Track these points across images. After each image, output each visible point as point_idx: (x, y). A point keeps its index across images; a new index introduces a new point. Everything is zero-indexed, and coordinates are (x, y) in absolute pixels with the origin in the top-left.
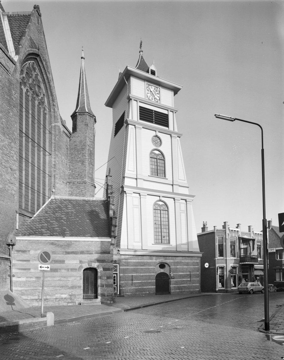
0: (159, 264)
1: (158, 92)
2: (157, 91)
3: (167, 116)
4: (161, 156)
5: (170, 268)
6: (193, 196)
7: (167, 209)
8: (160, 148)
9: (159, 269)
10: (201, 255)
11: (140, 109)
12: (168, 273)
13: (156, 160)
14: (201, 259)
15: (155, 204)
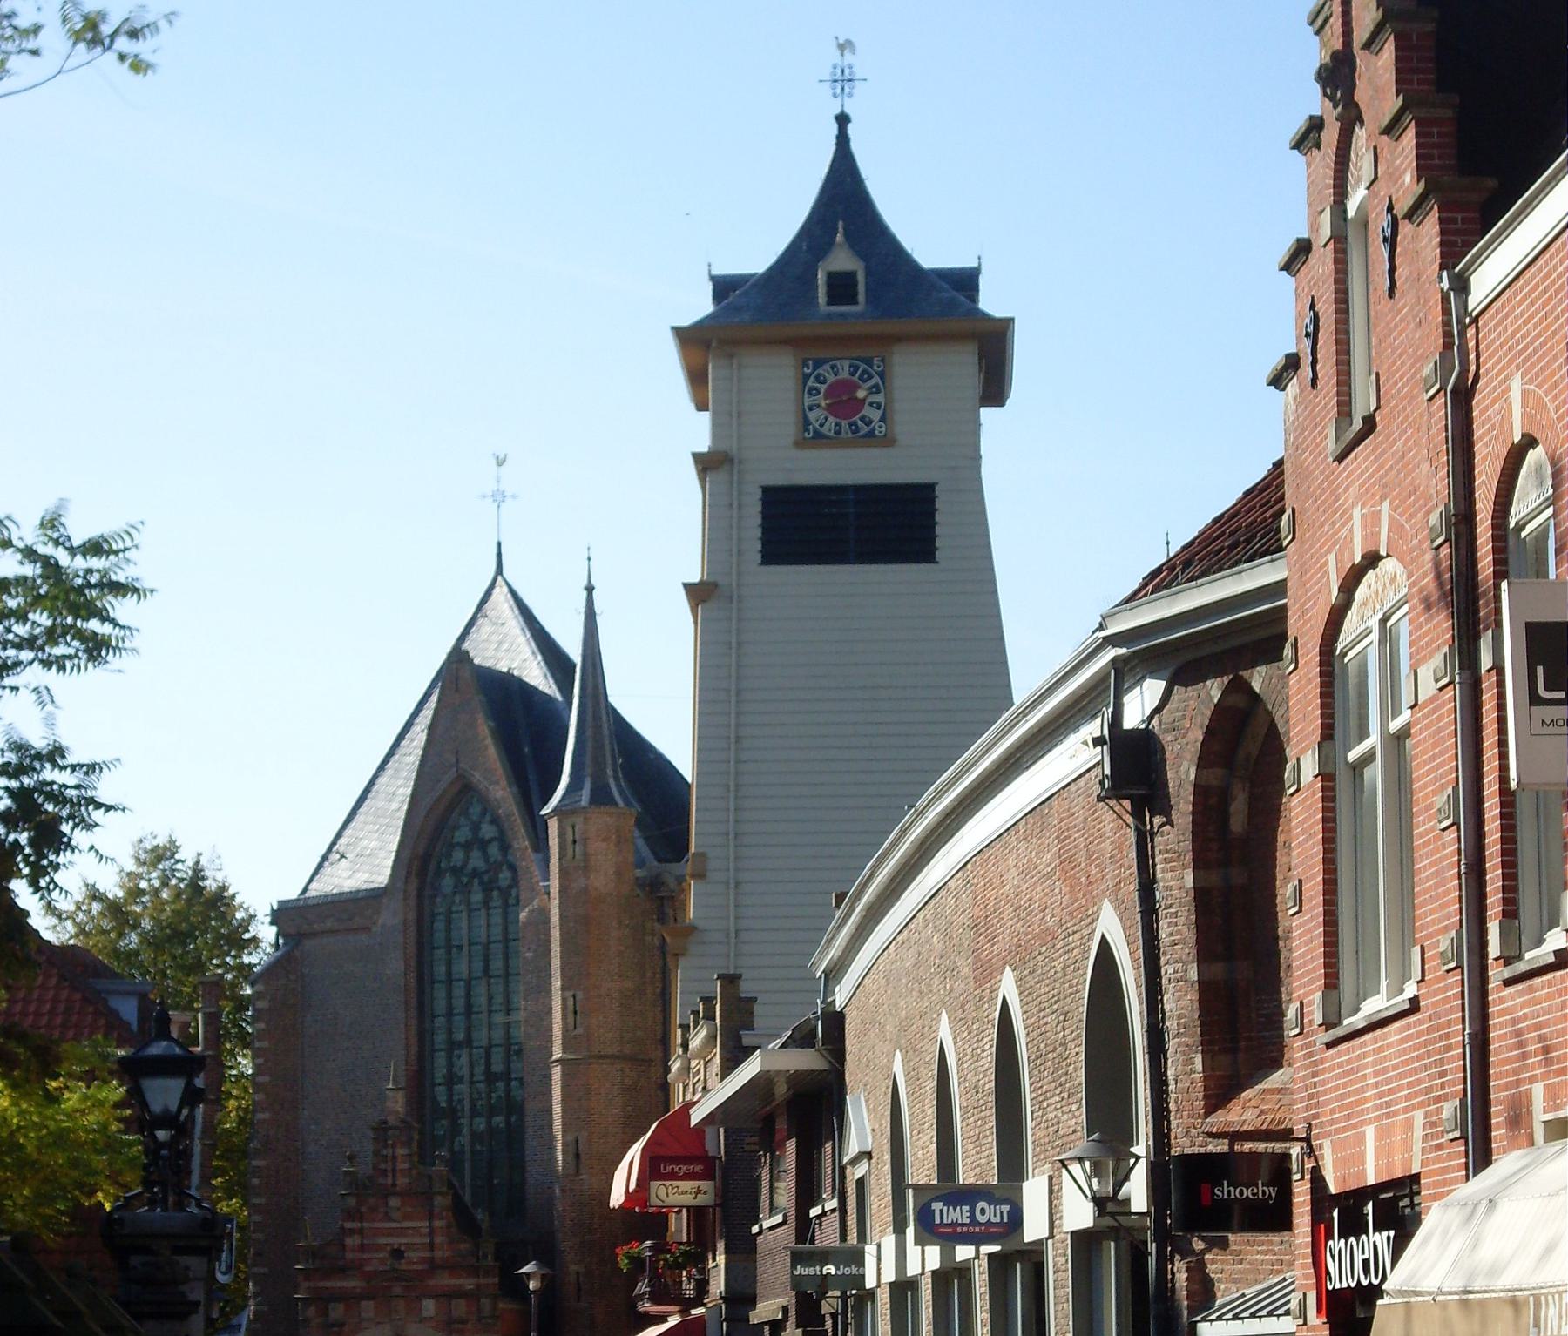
1: (876, 379)
2: (871, 377)
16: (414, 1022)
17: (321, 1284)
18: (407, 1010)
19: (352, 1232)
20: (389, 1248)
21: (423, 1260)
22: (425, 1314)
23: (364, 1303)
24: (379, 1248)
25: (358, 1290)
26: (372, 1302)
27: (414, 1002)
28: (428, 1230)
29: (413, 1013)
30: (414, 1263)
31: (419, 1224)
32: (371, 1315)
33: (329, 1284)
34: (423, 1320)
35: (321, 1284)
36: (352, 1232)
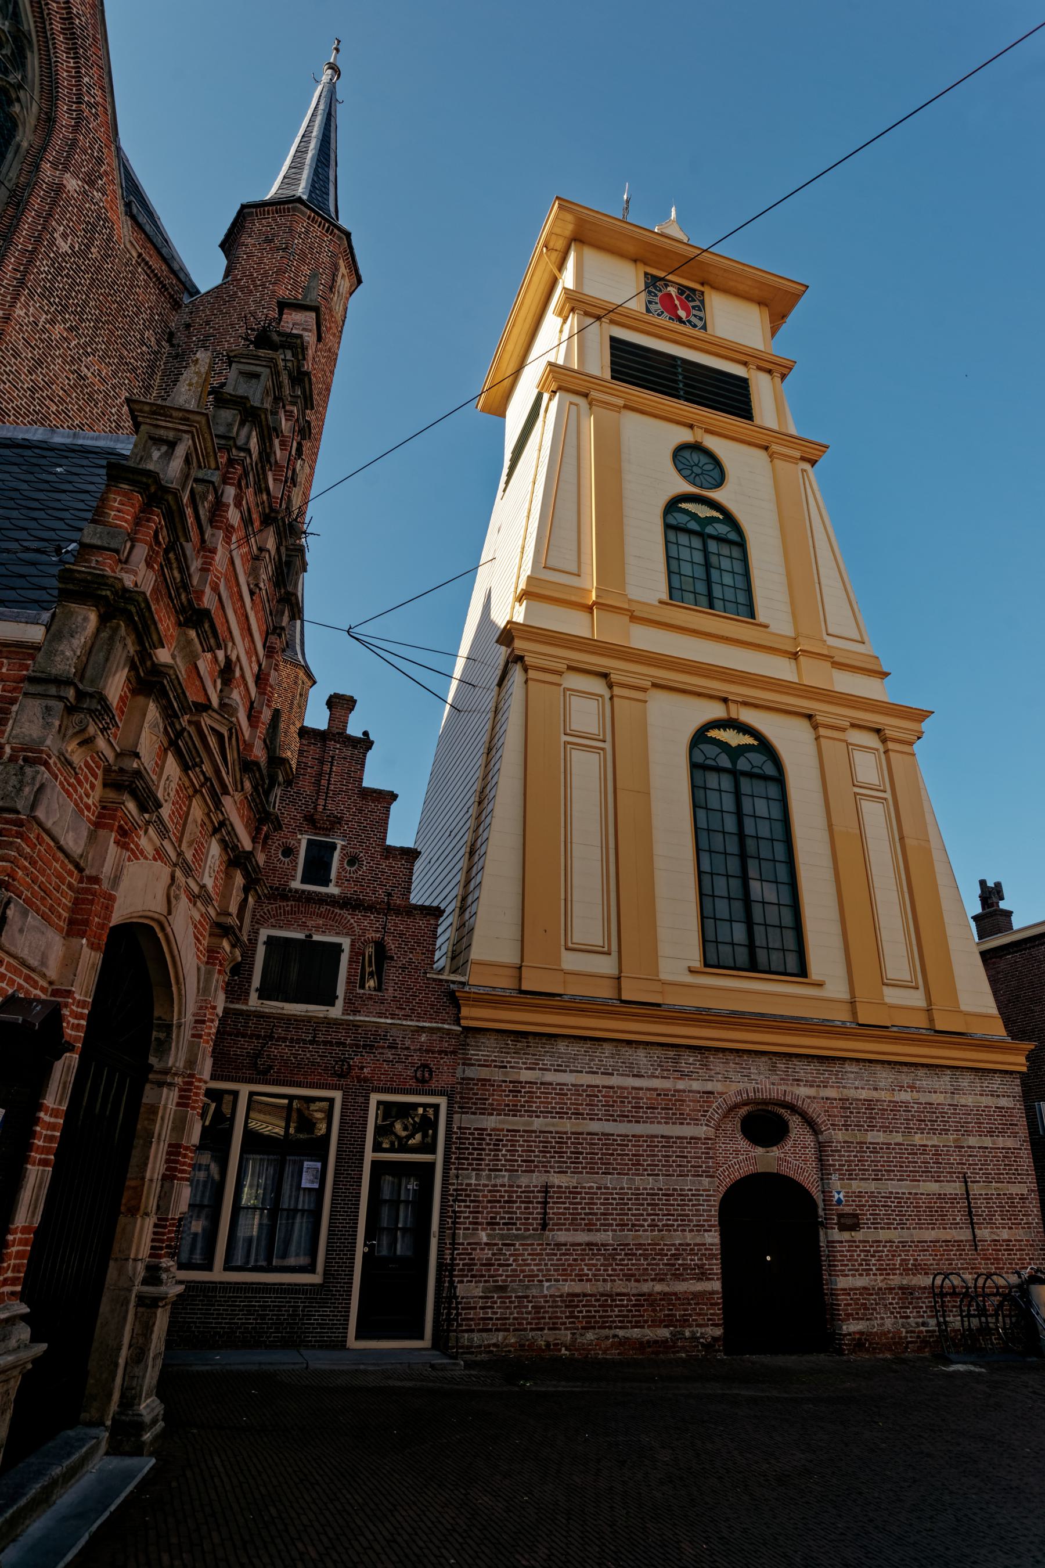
0: (743, 1111)
3: (743, 384)
4: (722, 529)
5: (822, 1148)
6: (922, 715)
7: (769, 770)
8: (715, 495)
9: (743, 1144)
10: (1022, 1060)
11: (612, 347)
12: (808, 1177)
13: (697, 543)
14: (1023, 1084)
15: (700, 737)
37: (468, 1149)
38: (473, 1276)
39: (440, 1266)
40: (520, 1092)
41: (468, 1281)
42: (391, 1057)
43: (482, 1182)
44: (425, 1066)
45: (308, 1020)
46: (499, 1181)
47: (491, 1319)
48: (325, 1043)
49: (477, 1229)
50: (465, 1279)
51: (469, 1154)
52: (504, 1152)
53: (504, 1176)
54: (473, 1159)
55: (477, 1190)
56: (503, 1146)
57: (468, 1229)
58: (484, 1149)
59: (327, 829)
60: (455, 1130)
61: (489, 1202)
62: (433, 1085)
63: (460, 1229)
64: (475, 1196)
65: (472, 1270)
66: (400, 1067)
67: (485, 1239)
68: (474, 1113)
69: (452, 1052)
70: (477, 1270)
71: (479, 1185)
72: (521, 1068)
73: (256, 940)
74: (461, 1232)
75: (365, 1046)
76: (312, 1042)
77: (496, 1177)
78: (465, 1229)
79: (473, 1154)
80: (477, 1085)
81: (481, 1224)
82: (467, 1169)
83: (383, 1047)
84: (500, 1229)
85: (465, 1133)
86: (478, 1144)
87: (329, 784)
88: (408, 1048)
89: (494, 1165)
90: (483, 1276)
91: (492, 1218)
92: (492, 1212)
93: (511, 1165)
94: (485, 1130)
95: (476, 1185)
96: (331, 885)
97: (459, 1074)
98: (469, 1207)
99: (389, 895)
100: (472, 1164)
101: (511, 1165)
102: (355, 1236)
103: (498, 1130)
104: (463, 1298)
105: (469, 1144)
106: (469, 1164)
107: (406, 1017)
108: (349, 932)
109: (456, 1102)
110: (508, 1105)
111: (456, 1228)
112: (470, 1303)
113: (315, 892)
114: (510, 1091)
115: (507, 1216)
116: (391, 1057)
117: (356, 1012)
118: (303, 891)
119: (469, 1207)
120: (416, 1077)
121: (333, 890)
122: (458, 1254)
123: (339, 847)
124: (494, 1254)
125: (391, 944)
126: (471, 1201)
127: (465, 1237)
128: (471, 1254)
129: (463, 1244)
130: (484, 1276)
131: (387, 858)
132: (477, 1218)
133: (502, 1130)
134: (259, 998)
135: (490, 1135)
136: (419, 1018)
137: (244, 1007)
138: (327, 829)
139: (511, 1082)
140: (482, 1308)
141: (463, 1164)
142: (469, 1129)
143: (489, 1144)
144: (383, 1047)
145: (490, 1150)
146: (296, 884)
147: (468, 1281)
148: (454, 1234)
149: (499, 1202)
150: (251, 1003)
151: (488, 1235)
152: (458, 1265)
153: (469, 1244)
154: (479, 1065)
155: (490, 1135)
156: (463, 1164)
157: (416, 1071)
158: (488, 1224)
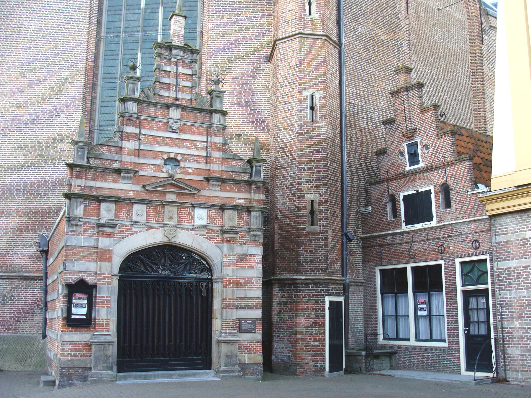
16: (94, 33)
17: (92, 183)
18: (90, 24)
19: (131, 136)
20: (165, 157)
21: (197, 171)
22: (197, 222)
23: (136, 207)
24: (157, 154)
25: (131, 194)
26: (145, 206)
27: (95, 20)
28: (205, 144)
29: (94, 27)
30: (190, 174)
31: (199, 138)
32: (143, 219)
33: (99, 184)
34: (195, 228)
35: (92, 183)
36: (131, 136)
37: (503, 279)
38: (514, 344)
39: (495, 339)
40: (527, 244)
41: (512, 347)
42: (460, 239)
43: (513, 296)
44: (476, 241)
45: (424, 229)
46: (522, 295)
47: (526, 366)
48: (433, 239)
49: (513, 321)
50: (511, 346)
51: (504, 282)
52: (522, 279)
53: (524, 292)
54: (507, 285)
55: (511, 301)
56: (522, 275)
57: (509, 321)
58: (512, 279)
59: (410, 137)
60: (496, 271)
61: (518, 306)
62: (481, 249)
63: (505, 321)
64: (510, 304)
65: (514, 341)
66: (465, 243)
67: (518, 325)
68: (504, 260)
69: (487, 231)
70: (516, 341)
71: (512, 298)
72: (526, 231)
73: (400, 199)
74: (506, 322)
75: (448, 237)
76: (428, 240)
77: (520, 292)
78: (507, 321)
79: (506, 282)
80: (504, 245)
81: (515, 318)
82: (505, 290)
83: (456, 236)
84: (525, 320)
85: (501, 272)
86: (509, 276)
87: (405, 114)
88: (466, 234)
89: (518, 287)
90: (520, 344)
91: (520, 314)
92: (520, 312)
93: (527, 286)
94: (511, 268)
95: (510, 298)
96: (420, 162)
97: (494, 241)
98: (508, 309)
99: (444, 157)
100: (507, 287)
101: (527, 286)
102: (457, 326)
103: (518, 267)
104: (510, 355)
105: (504, 277)
106: (505, 287)
107: (464, 217)
108: (431, 182)
109: (494, 256)
110: (521, 253)
111: (502, 320)
112: (514, 357)
113: (415, 169)
114: (521, 245)
115: (528, 313)
116: (460, 239)
117: (442, 221)
118: (411, 170)
119: (508, 309)
120: (473, 247)
121: (421, 165)
122: (505, 333)
123: (419, 143)
124: (524, 333)
125: (450, 182)
126: (509, 306)
127: (508, 324)
128: (512, 333)
129: (507, 328)
130: (520, 344)
131: (439, 139)
132: (513, 315)
133: (520, 267)
134: (406, 225)
135: (514, 271)
136: (470, 216)
137: (399, 231)
138: (410, 137)
139: (521, 240)
140: (521, 360)
141: (502, 288)
142: (503, 269)
143: (514, 276)
144: (456, 236)
145: (515, 279)
146: (408, 168)
147: (512, 347)
148: (502, 324)
149: (523, 306)
150: (403, 228)
151: (520, 323)
152: (506, 338)
153: (510, 328)
154: (503, 234)
155: (514, 271)
156: (502, 288)
157: (472, 244)
158: (519, 318)
